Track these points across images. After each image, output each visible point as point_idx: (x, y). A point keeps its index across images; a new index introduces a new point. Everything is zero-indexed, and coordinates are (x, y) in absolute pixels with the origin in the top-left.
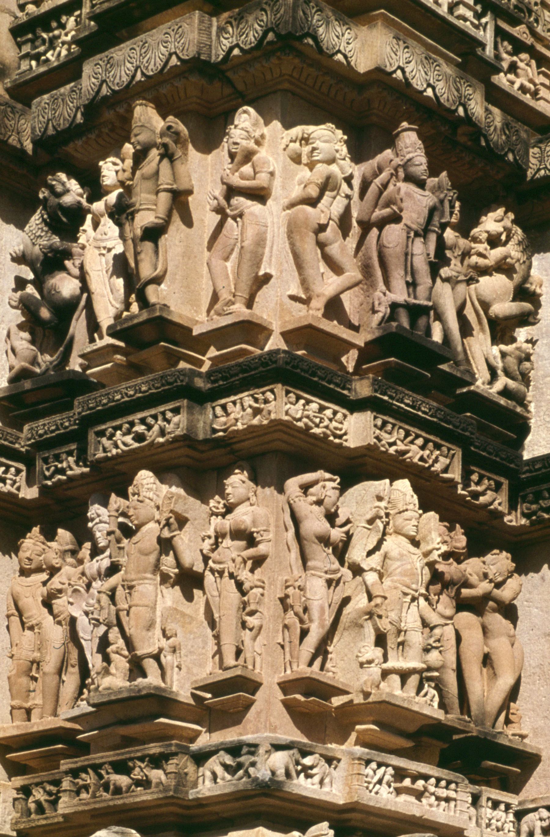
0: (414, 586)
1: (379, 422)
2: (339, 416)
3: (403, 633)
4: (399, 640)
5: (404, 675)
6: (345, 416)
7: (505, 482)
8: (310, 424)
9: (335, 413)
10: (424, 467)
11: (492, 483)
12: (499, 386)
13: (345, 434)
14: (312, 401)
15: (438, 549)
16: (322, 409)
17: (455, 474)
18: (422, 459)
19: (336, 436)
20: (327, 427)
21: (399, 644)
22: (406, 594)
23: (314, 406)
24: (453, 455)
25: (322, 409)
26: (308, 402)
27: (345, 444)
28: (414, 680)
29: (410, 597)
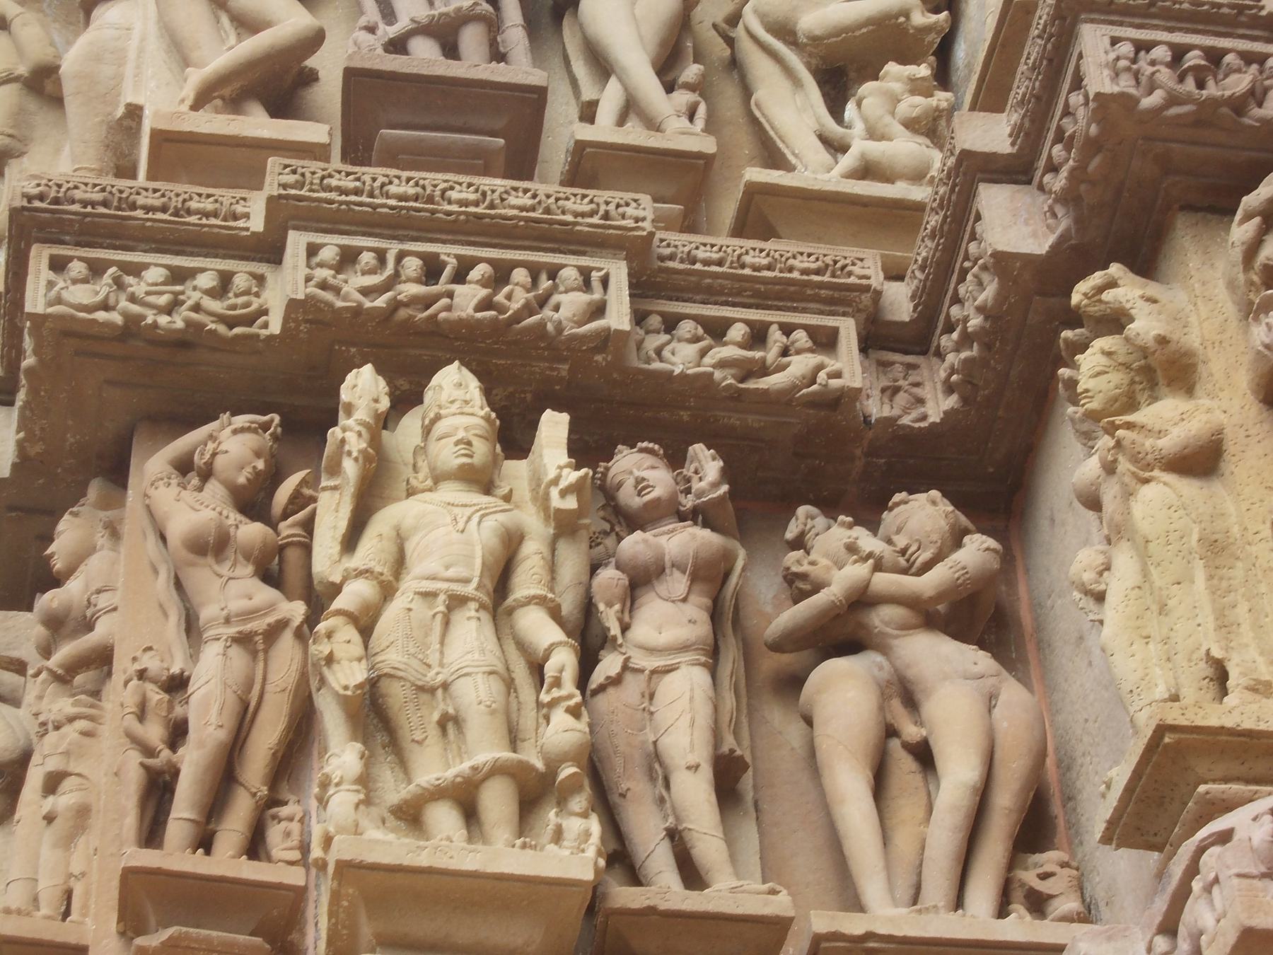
0: (451, 573)
1: (328, 255)
2: (240, 281)
3: (440, 692)
4: (436, 716)
5: (466, 800)
6: (260, 279)
7: (848, 329)
8: (135, 309)
9: (226, 279)
10: (494, 321)
11: (801, 337)
12: (847, 161)
13: (264, 312)
14: (146, 266)
15: (555, 482)
16: (179, 276)
17: (619, 317)
18: (486, 304)
19: (231, 323)
20: (197, 308)
21: (442, 724)
22: (429, 595)
23: (154, 274)
24: (605, 282)
25: (179, 276)
26: (136, 270)
27: (264, 333)
28: (497, 802)
29: (442, 597)
